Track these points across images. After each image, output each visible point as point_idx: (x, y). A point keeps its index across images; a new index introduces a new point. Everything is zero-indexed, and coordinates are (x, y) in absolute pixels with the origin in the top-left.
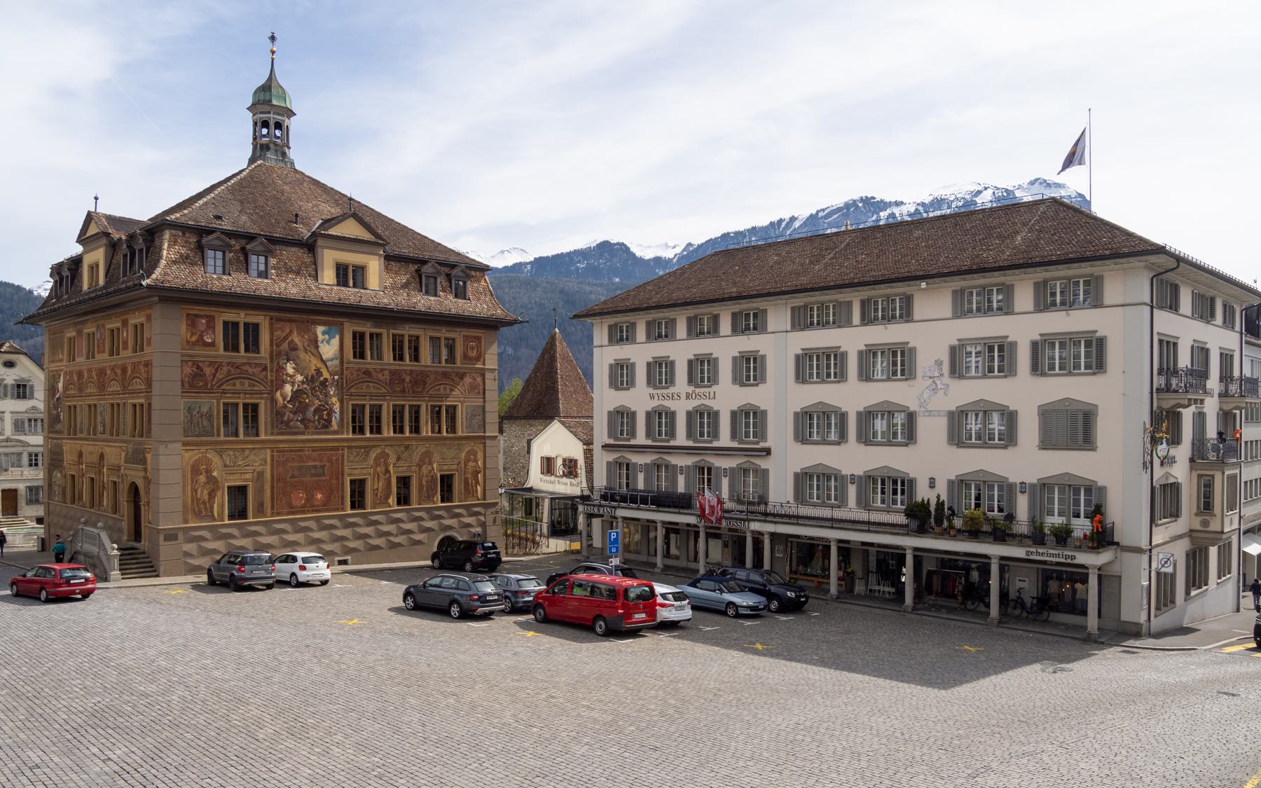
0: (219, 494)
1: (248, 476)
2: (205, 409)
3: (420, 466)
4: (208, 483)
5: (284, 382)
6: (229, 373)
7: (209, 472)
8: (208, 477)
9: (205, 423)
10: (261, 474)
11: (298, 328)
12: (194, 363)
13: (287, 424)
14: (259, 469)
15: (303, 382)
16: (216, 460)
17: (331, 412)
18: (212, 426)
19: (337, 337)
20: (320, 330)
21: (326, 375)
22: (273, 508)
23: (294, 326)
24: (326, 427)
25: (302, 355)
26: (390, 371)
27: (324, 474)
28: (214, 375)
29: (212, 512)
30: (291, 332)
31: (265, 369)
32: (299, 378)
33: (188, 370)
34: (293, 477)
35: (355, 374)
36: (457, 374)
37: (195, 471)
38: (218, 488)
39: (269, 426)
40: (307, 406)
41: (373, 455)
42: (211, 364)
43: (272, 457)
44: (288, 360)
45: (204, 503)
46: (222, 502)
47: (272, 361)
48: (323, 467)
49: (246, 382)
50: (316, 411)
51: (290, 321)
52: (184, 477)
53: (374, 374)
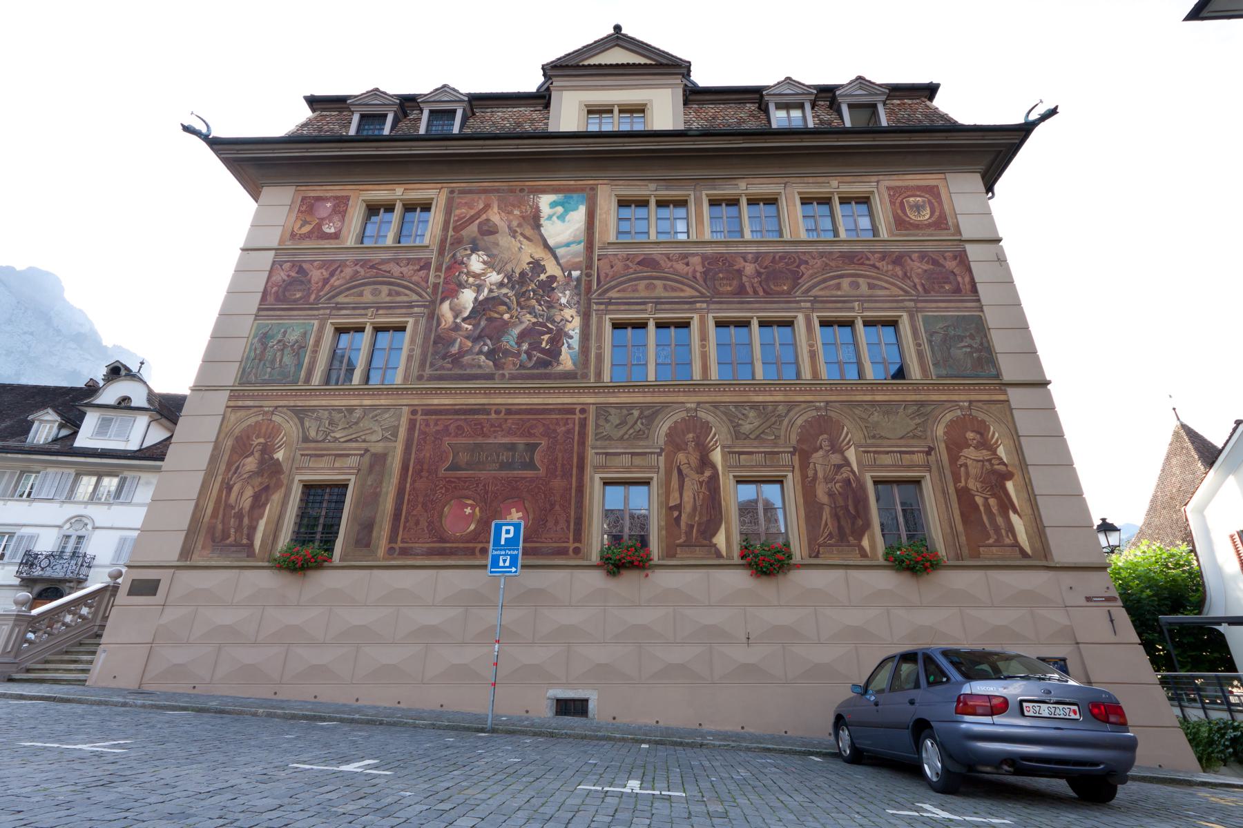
0: (276, 497)
1: (352, 462)
2: (293, 337)
3: (804, 454)
4: (259, 472)
5: (461, 286)
6: (353, 278)
7: (267, 450)
8: (262, 462)
9: (288, 360)
10: (378, 461)
11: (500, 200)
12: (294, 264)
13: (456, 360)
14: (378, 448)
15: (501, 285)
16: (289, 428)
17: (558, 337)
18: (299, 365)
19: (582, 211)
20: (545, 201)
21: (552, 269)
22: (393, 538)
23: (494, 199)
24: (546, 364)
25: (504, 240)
26: (704, 257)
27: (531, 465)
28: (326, 281)
29: (251, 537)
30: (487, 207)
31: (426, 266)
32: (494, 277)
33: (281, 276)
34: (454, 467)
35: (619, 266)
36: (884, 256)
37: (242, 446)
38: (278, 485)
39: (415, 364)
40: (506, 323)
41: (663, 428)
42: (324, 264)
43: (412, 425)
44: (474, 250)
45: (240, 516)
46: (280, 521)
47: (441, 252)
48: (532, 448)
49: (385, 289)
50: (522, 336)
51: (485, 191)
52: (213, 459)
53: (664, 263)
